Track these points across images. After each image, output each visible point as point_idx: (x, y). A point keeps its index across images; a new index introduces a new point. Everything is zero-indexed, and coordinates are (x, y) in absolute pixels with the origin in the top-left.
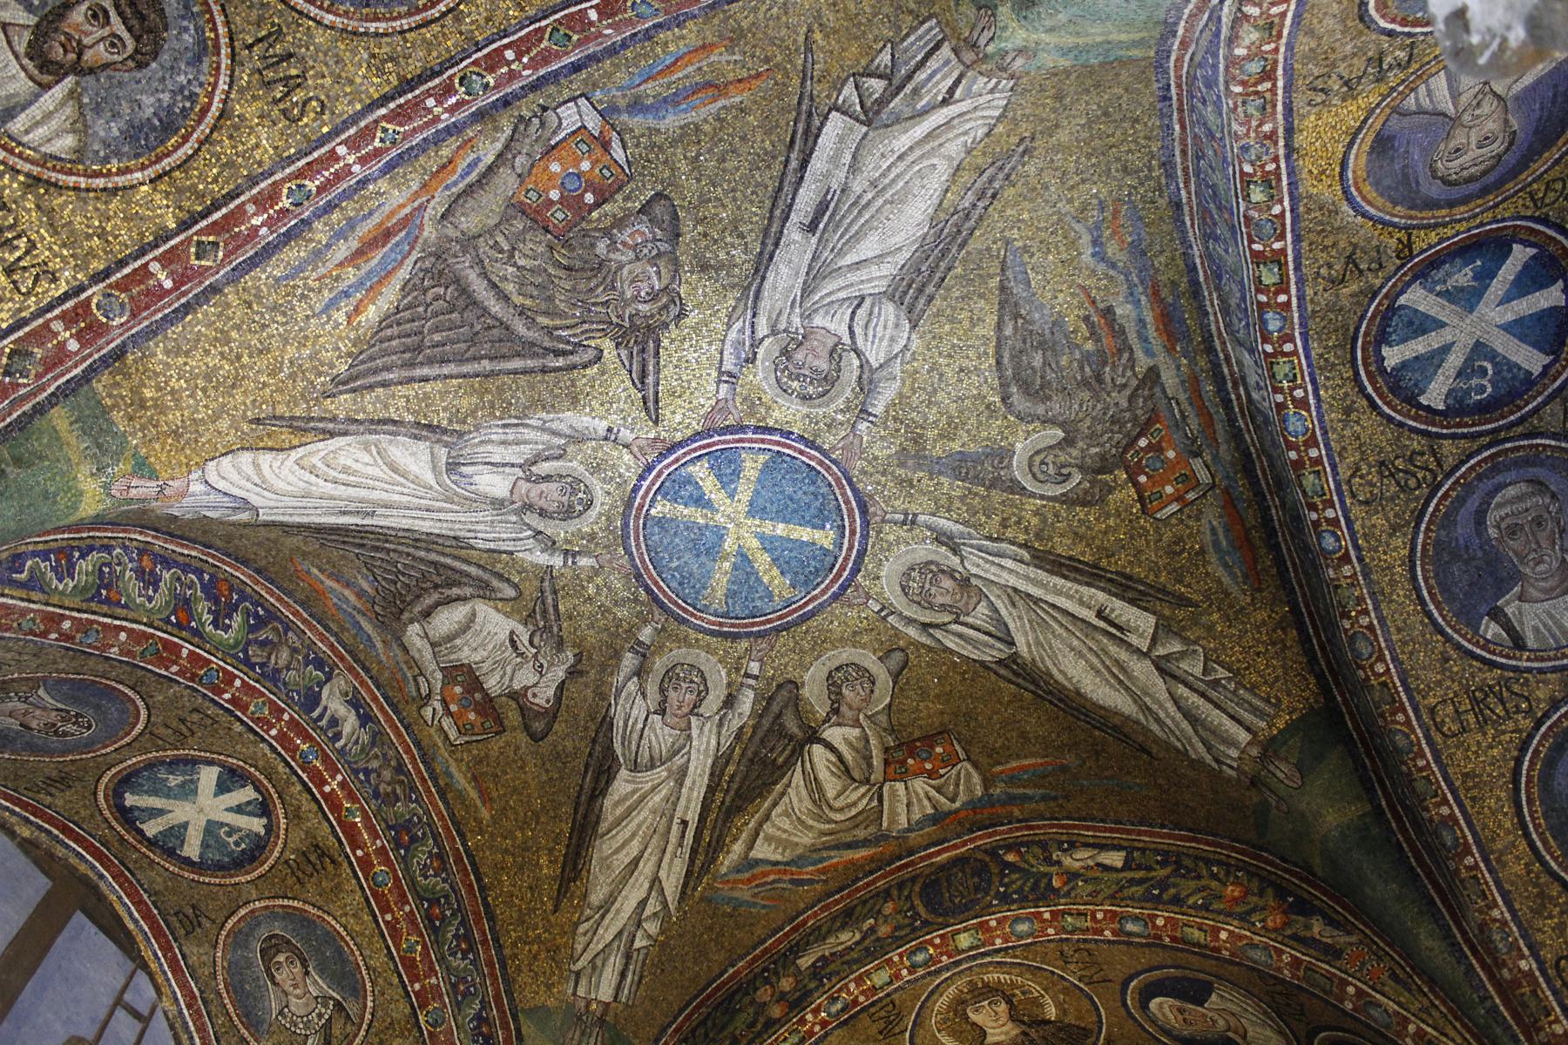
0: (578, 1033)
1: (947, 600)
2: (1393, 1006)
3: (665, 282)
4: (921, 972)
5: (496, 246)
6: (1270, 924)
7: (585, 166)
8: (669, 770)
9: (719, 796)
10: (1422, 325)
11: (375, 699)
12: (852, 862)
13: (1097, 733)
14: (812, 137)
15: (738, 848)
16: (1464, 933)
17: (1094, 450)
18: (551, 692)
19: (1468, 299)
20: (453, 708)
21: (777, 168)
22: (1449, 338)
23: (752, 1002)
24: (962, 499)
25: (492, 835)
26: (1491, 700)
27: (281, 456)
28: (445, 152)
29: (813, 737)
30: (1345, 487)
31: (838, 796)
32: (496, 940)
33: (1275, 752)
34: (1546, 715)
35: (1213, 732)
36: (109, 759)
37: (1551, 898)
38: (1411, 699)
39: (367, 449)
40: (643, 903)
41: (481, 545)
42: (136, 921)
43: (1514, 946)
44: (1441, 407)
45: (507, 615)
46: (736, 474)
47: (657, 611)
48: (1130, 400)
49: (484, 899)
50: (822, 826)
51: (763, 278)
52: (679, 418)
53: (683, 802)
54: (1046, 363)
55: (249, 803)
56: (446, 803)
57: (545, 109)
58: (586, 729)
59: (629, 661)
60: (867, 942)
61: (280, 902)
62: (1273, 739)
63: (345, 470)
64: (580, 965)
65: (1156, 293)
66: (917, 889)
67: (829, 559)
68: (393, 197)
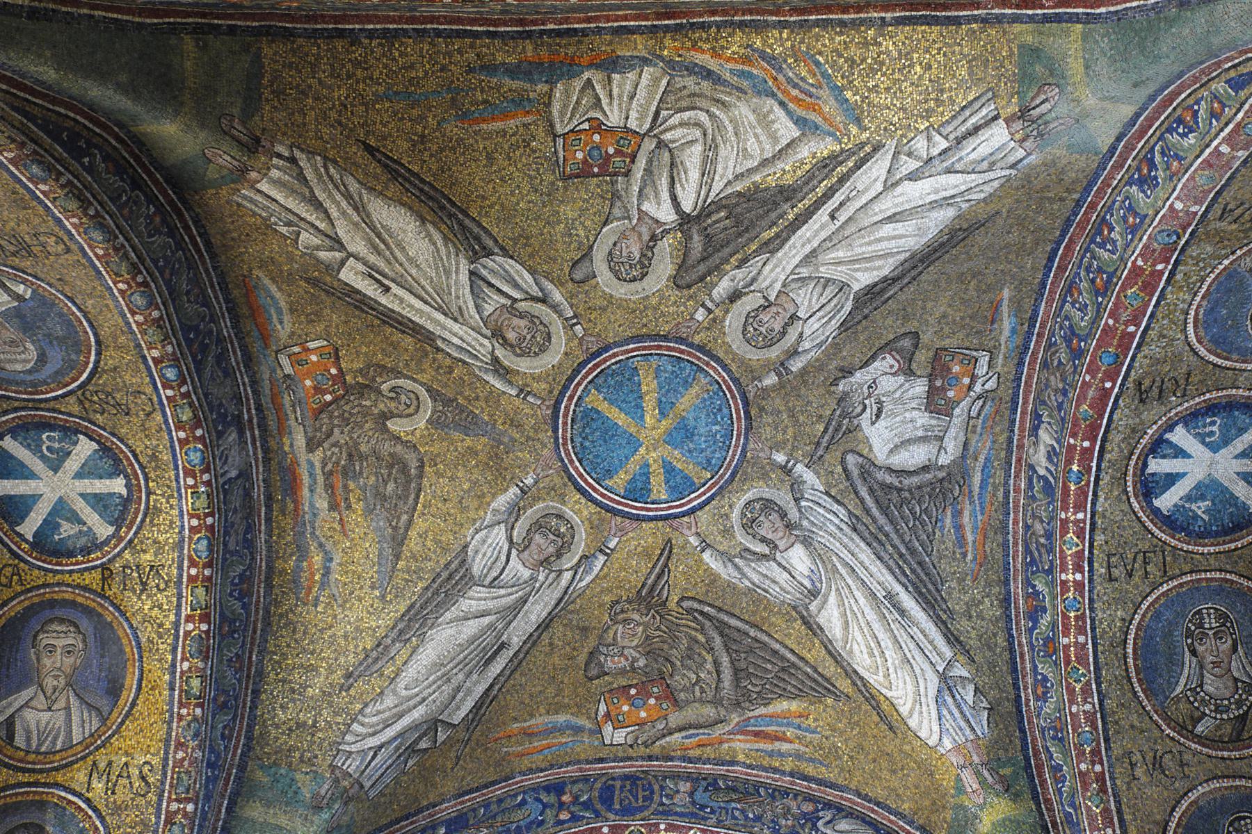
0: (1052, 126)
1: (516, 321)
3: (614, 628)
5: (702, 691)
7: (626, 708)
8: (817, 270)
10: (98, 501)
11: (1024, 413)
14: (478, 707)
17: (367, 403)
19: (61, 510)
21: (508, 685)
22: (77, 483)
24: (477, 398)
27: (895, 702)
28: (698, 752)
29: (685, 220)
39: (851, 652)
40: (913, 177)
41: (842, 512)
44: (81, 437)
46: (633, 480)
47: (751, 396)
48: (330, 434)
51: (550, 614)
52: (649, 536)
53: (824, 234)
54: (385, 483)
57: (631, 746)
58: (865, 328)
59: (796, 365)
63: (872, 655)
64: (1007, 172)
67: (600, 381)
68: (741, 746)
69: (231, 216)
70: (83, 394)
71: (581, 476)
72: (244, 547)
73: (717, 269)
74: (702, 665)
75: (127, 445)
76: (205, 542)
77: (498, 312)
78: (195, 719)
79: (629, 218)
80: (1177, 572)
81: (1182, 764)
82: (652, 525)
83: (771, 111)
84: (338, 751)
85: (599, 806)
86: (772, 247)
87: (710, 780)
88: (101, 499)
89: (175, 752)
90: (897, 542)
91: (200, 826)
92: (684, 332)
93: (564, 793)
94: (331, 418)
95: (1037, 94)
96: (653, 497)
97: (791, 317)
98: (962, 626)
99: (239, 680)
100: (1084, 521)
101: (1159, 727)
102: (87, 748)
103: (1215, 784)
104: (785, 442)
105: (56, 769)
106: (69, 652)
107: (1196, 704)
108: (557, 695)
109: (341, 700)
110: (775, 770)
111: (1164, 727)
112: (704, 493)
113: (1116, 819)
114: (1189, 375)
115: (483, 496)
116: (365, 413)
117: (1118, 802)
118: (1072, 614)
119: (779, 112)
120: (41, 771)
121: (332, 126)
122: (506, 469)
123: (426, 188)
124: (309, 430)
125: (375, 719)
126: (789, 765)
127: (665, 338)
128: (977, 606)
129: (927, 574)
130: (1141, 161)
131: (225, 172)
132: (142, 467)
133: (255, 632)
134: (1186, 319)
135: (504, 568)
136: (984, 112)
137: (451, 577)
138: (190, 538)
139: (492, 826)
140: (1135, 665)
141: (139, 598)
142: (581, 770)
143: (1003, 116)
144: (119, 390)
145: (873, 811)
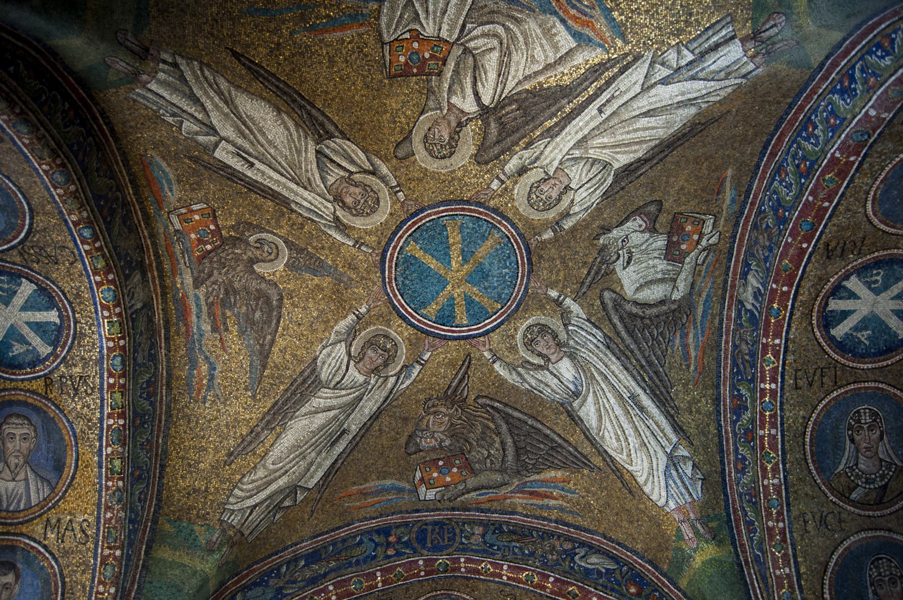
0: (778, 46)
3: (427, 418)
5: (492, 463)
7: (435, 475)
8: (587, 152)
11: (737, 261)
14: (326, 475)
18: (629, 224)
24: (323, 248)
28: (487, 506)
29: (485, 111)
31: (491, 50)
39: (603, 437)
40: (665, 81)
41: (599, 334)
44: (24, 280)
45: (619, 282)
46: (442, 309)
47: (533, 247)
48: (210, 275)
50: (515, 29)
51: (379, 408)
53: (593, 125)
54: (254, 311)
57: (439, 501)
58: (622, 197)
59: (568, 224)
63: (618, 440)
67: (417, 235)
68: (519, 500)
69: (129, 109)
70: (23, 248)
71: (402, 306)
72: (149, 361)
73: (509, 150)
74: (492, 444)
75: (57, 287)
76: (119, 359)
77: (338, 182)
78: (118, 489)
79: (441, 109)
80: (845, 382)
81: (840, 521)
82: (456, 343)
83: (554, 26)
84: (225, 509)
85: (416, 545)
86: (551, 134)
87: (497, 525)
88: (41, 327)
89: (105, 513)
90: (640, 357)
91: (126, 565)
93: (391, 535)
94: (211, 262)
95: (768, 20)
96: (457, 322)
97: (565, 188)
98: (685, 419)
99: (150, 459)
100: (780, 345)
101: (825, 495)
102: (42, 508)
103: (863, 535)
104: (557, 282)
105: (21, 523)
106: (25, 439)
107: (852, 478)
108: (384, 466)
109: (227, 472)
110: (544, 519)
111: (829, 494)
112: (496, 320)
113: (792, 561)
114: (864, 238)
115: (328, 321)
116: (237, 259)
117: (794, 549)
118: (768, 413)
119: (560, 27)
120: (11, 524)
121: (207, 37)
122: (346, 301)
123: (281, 86)
125: (250, 486)
126: (554, 515)
127: (468, 202)
128: (696, 404)
129: (661, 381)
130: (843, 76)
131: (122, 76)
132: (70, 303)
133: (160, 422)
134: (867, 198)
135: (345, 375)
136: (724, 32)
137: (304, 381)
138: (108, 356)
139: (338, 560)
140: (811, 450)
141: (73, 400)
142: (402, 518)
143: (739, 36)
144: (49, 246)
145: (615, 549)
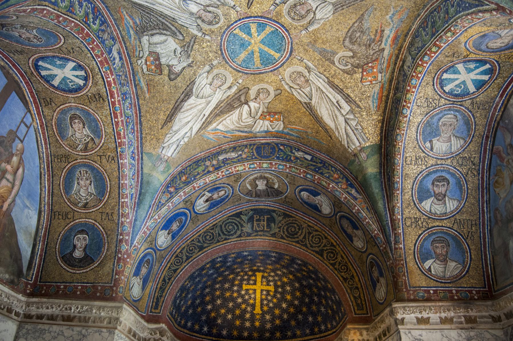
1: (300, 83)
2: (365, 215)
4: (251, 169)
6: (343, 187)
9: (216, 110)
11: (124, 53)
12: (240, 136)
13: (320, 128)
15: (214, 125)
16: (388, 206)
17: (357, 62)
18: (180, 69)
19: (469, 71)
20: (148, 63)
22: (459, 77)
23: (204, 165)
25: (148, 102)
26: (420, 160)
29: (246, 103)
30: (415, 101)
32: (141, 131)
33: (363, 151)
34: (429, 167)
35: (351, 140)
36: (41, 51)
37: (411, 206)
38: (403, 153)
40: (186, 133)
41: (180, 22)
42: (29, 98)
43: (399, 213)
45: (177, 43)
46: (263, 30)
49: (140, 119)
54: (360, 37)
55: (81, 76)
56: (136, 89)
58: (187, 82)
59: (207, 68)
60: (239, 158)
61: (81, 106)
62: (364, 147)
65: (397, 31)
66: (255, 147)
67: (274, 61)
71: (283, 32)
86: (221, 102)
92: (246, 76)
94: (372, 58)
116: (359, 58)
124: (381, 55)
